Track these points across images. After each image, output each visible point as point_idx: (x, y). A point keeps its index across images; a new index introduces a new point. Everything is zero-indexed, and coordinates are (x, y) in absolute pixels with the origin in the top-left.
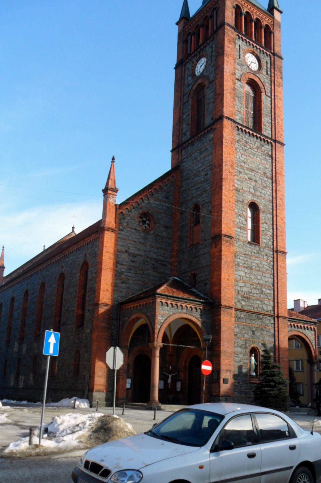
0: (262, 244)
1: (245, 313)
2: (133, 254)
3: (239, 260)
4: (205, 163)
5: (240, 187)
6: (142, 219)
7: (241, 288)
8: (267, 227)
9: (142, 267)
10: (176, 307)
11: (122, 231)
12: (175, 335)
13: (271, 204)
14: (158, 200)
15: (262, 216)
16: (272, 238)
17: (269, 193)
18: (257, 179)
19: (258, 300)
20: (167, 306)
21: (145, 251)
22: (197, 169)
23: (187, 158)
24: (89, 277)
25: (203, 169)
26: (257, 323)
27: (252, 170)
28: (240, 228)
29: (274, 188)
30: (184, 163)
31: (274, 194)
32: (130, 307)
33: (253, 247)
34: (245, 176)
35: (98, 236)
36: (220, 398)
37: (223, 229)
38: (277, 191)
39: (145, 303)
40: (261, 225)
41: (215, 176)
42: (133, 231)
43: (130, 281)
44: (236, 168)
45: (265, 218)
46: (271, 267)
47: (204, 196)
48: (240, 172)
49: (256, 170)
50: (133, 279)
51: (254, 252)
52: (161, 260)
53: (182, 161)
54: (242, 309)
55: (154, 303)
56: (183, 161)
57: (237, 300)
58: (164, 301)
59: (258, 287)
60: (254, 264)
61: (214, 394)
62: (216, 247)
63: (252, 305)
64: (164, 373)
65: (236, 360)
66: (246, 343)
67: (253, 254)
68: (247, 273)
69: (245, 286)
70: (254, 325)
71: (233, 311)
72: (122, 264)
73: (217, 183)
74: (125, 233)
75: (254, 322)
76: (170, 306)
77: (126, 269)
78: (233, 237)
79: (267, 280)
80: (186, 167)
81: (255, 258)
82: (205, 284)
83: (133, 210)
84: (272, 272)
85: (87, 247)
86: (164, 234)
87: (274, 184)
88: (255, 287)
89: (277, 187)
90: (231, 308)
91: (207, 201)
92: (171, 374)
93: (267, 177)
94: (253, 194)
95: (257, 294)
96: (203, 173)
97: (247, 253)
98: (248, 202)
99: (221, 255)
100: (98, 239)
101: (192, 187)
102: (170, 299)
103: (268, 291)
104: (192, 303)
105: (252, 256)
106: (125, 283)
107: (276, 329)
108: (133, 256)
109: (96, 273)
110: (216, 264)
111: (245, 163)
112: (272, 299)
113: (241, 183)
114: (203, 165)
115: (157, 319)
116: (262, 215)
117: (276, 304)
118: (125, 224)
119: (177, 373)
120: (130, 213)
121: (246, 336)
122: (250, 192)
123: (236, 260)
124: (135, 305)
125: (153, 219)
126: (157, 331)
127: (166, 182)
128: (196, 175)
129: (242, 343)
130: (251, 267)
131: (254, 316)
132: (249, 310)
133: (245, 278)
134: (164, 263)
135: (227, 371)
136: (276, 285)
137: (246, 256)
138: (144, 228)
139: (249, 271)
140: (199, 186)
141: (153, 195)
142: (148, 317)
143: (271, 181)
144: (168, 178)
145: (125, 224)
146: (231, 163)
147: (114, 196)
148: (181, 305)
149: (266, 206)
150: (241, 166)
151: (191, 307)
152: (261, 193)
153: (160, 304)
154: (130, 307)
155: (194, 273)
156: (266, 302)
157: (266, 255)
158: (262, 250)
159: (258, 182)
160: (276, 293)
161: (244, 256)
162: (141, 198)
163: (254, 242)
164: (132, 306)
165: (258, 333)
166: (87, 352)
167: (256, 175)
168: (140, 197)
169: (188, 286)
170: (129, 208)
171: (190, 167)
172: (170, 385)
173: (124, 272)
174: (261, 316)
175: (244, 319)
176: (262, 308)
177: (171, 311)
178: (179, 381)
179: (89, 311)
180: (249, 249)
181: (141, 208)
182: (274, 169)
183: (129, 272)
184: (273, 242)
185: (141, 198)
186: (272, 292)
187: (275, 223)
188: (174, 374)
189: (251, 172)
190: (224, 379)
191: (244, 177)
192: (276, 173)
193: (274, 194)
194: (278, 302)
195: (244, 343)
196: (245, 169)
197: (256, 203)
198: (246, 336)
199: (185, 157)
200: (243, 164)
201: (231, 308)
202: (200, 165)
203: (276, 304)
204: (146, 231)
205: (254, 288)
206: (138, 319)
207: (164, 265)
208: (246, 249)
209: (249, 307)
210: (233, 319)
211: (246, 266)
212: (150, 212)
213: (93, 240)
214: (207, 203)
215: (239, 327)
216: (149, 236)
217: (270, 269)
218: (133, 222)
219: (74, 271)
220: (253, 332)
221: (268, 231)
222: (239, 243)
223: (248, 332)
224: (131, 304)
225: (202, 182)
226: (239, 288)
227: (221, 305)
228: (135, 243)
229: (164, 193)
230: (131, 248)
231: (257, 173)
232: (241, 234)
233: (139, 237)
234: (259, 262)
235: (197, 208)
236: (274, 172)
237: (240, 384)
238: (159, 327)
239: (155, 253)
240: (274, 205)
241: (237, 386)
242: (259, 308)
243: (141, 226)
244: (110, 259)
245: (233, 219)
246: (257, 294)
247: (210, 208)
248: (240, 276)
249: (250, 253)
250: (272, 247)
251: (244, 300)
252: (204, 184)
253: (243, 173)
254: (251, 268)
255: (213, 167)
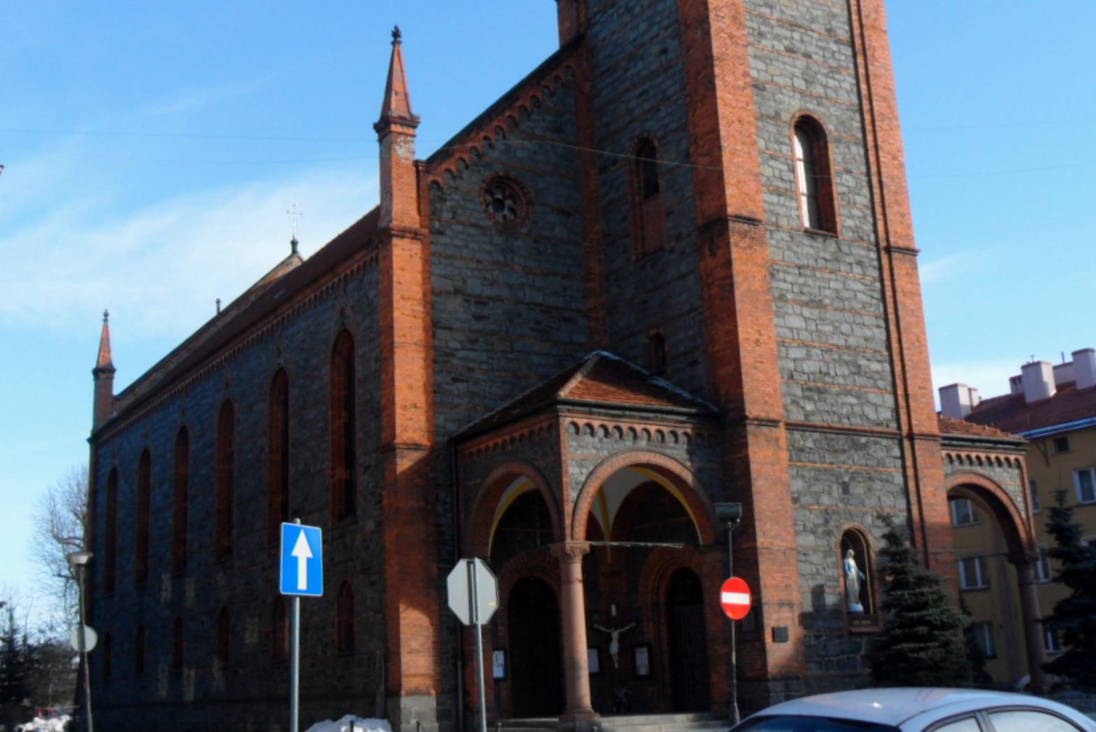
0: (845, 235)
1: (817, 436)
2: (479, 296)
3: (783, 285)
4: (658, 19)
5: (763, 77)
6: (492, 194)
7: (798, 363)
8: (851, 183)
9: (507, 332)
10: (617, 435)
11: (441, 233)
12: (620, 515)
13: (857, 117)
14: (531, 136)
15: (836, 155)
16: (869, 212)
17: (847, 86)
18: (811, 49)
19: (848, 393)
20: (593, 433)
21: (510, 286)
22: (635, 40)
23: (603, 11)
24: (359, 372)
25: (653, 38)
26: (853, 461)
27: (793, 26)
28: (778, 192)
29: (861, 71)
30: (597, 28)
31: (863, 87)
32: (483, 447)
33: (819, 243)
34: (776, 43)
35: (373, 254)
36: (770, 684)
37: (729, 200)
38: (871, 78)
39: (526, 431)
40: (835, 180)
41: (691, 52)
42: (471, 231)
43: (478, 375)
44: (749, 24)
45: (844, 159)
46: (877, 295)
47: (662, 114)
48: (761, 35)
49: (806, 24)
50: (485, 366)
51: (824, 259)
52: (557, 308)
53: (589, 25)
54: (807, 423)
55: (554, 427)
56: (592, 21)
57: (788, 401)
58: (581, 422)
59: (846, 357)
60: (828, 292)
61: (749, 674)
62: (713, 254)
63: (834, 409)
64: (596, 626)
65: (803, 572)
66: (827, 521)
67: (821, 263)
68: (809, 319)
69: (809, 357)
70: (846, 466)
71: (781, 432)
72: (450, 329)
73: (698, 73)
74: (448, 241)
75: (843, 457)
76: (601, 433)
77: (461, 342)
78: (760, 221)
79: (868, 333)
80: (602, 35)
81: (827, 275)
82: (694, 363)
83: (466, 174)
84: (882, 310)
85: (345, 291)
86: (560, 232)
87: (860, 60)
88: (836, 356)
89: (870, 67)
90: (773, 423)
91: (673, 126)
92: (616, 628)
93: (838, 42)
94: (802, 93)
95: (843, 376)
96: (655, 49)
97: (805, 262)
98: (793, 117)
99: (730, 277)
100: (374, 263)
101: (627, 90)
102: (600, 414)
103: (875, 366)
104: (663, 420)
105: (820, 269)
106: (463, 381)
107: (910, 472)
108: (477, 303)
109: (377, 359)
110: (717, 302)
111: (771, 7)
112: (889, 388)
113: (767, 64)
114: (651, 25)
115: (567, 472)
116: (837, 150)
117: (902, 402)
118: (446, 215)
119: (633, 625)
120: (458, 182)
121: (825, 500)
122: (794, 89)
123: (775, 284)
124: (499, 441)
125: (525, 194)
126: (568, 508)
127: (551, 86)
128: (633, 58)
129: (816, 521)
130: (820, 301)
131: (841, 441)
132: (825, 424)
133: (805, 336)
134: (567, 314)
135: (781, 604)
136: (895, 345)
137: (802, 271)
138: (501, 220)
139: (816, 312)
140: (647, 86)
141: (516, 125)
142: (539, 471)
143: (849, 52)
144: (554, 74)
145: (446, 215)
146: (733, 12)
147: (409, 138)
148: (632, 429)
149: (842, 123)
150: (760, 15)
151: (659, 431)
152: (825, 87)
153: (572, 429)
154: (483, 447)
155: (658, 334)
156: (873, 398)
157: (860, 263)
158: (845, 249)
159: (815, 57)
160: (898, 369)
161: (796, 271)
162: (486, 138)
163: (820, 227)
164: (491, 444)
165: (858, 489)
166: (373, 584)
167: (806, 39)
168: (482, 134)
169: (645, 372)
170: (453, 168)
171: (614, 38)
172: (615, 659)
173: (457, 350)
174: (863, 440)
175: (814, 453)
176: (863, 416)
177: (602, 448)
178: (641, 645)
179: (367, 468)
180: (809, 250)
181: (488, 166)
182: (855, 17)
183: (470, 350)
184: (875, 225)
185: (486, 138)
186: (887, 367)
187: (874, 169)
188: (627, 628)
189: (792, 31)
190: (773, 630)
191: (773, 47)
192: (861, 26)
193: (863, 87)
194: (906, 396)
195: (821, 521)
196: (774, 23)
197: (816, 116)
198: (825, 500)
199: (596, 9)
200: (766, 11)
201: (773, 423)
202: (643, 27)
203: (902, 402)
204: (507, 229)
205: (834, 360)
206: (508, 479)
207: (567, 320)
208: (799, 250)
209: (826, 417)
210: (784, 455)
211: (805, 298)
212: (512, 174)
213: (359, 268)
214: (675, 130)
215: (803, 477)
216: (519, 243)
217: (874, 301)
218: (469, 205)
219: (314, 361)
220: (845, 488)
221: (858, 194)
222: (778, 235)
223: (830, 487)
224: (485, 437)
225: (654, 74)
226: (791, 365)
227: (746, 418)
228: (480, 266)
229: (549, 118)
230: (469, 281)
231: (809, 33)
232: (782, 211)
233: (489, 248)
234: (839, 286)
235: (645, 147)
236: (856, 24)
237: (824, 638)
238: (574, 495)
239: (538, 289)
240: (867, 117)
241: (814, 645)
242: (855, 417)
243: (491, 217)
244: (415, 317)
245: (756, 170)
246: (843, 376)
247: (684, 146)
248: (791, 329)
249: (811, 263)
250: (872, 238)
251: (809, 399)
252: (658, 80)
253: (769, 36)
254: (819, 305)
255: (682, 28)
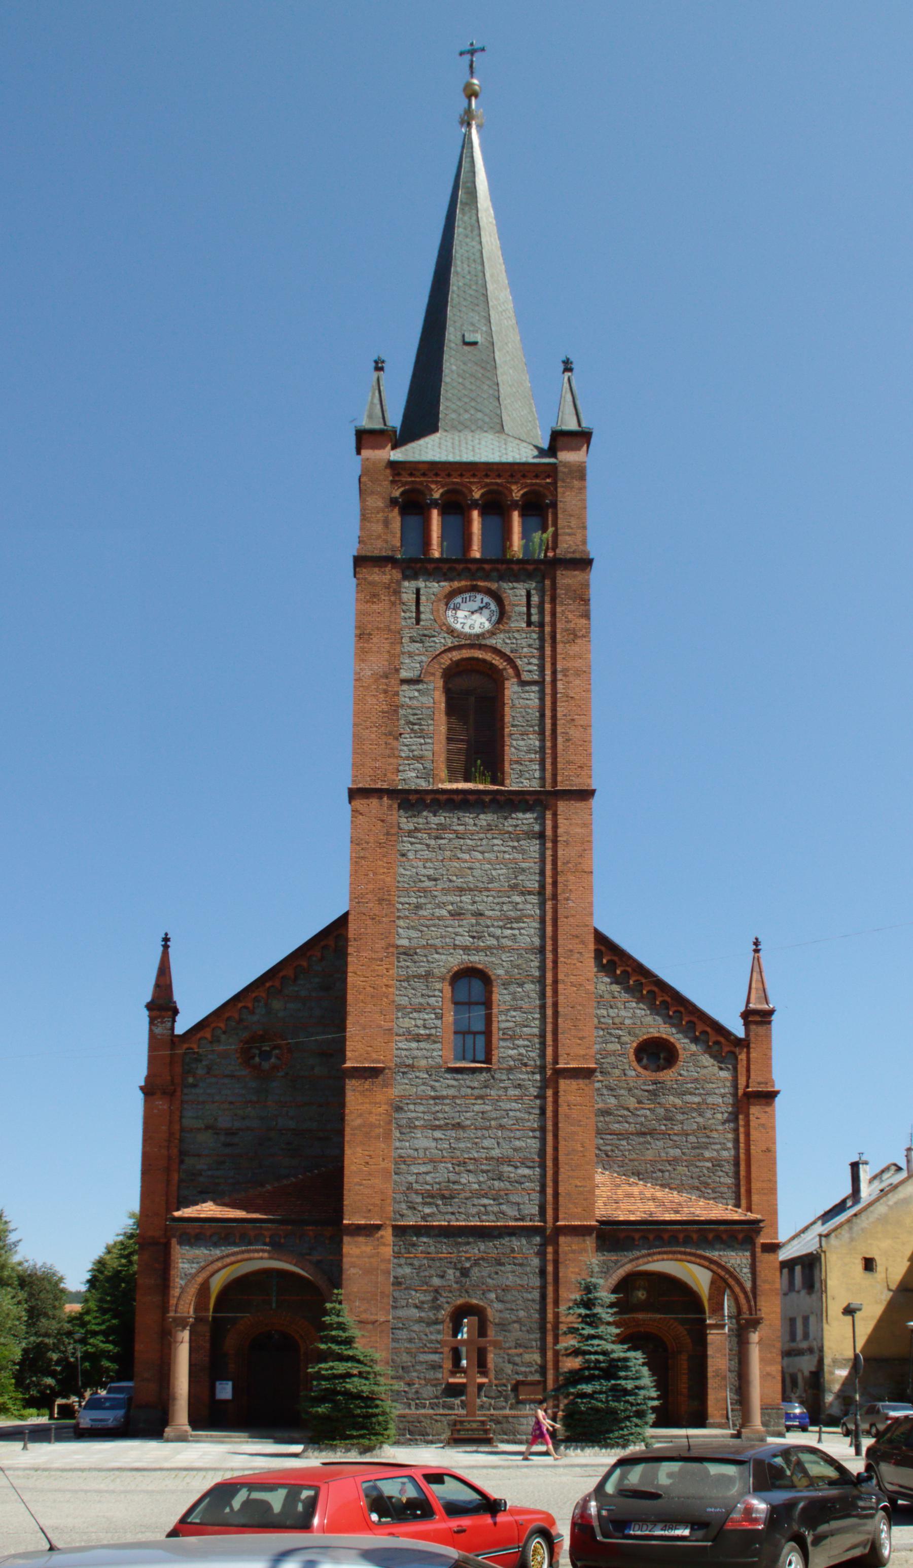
42: (226, 1081)
139: (453, 1133)
198: (436, 1281)
232: (419, 1053)
254: (458, 1126)
